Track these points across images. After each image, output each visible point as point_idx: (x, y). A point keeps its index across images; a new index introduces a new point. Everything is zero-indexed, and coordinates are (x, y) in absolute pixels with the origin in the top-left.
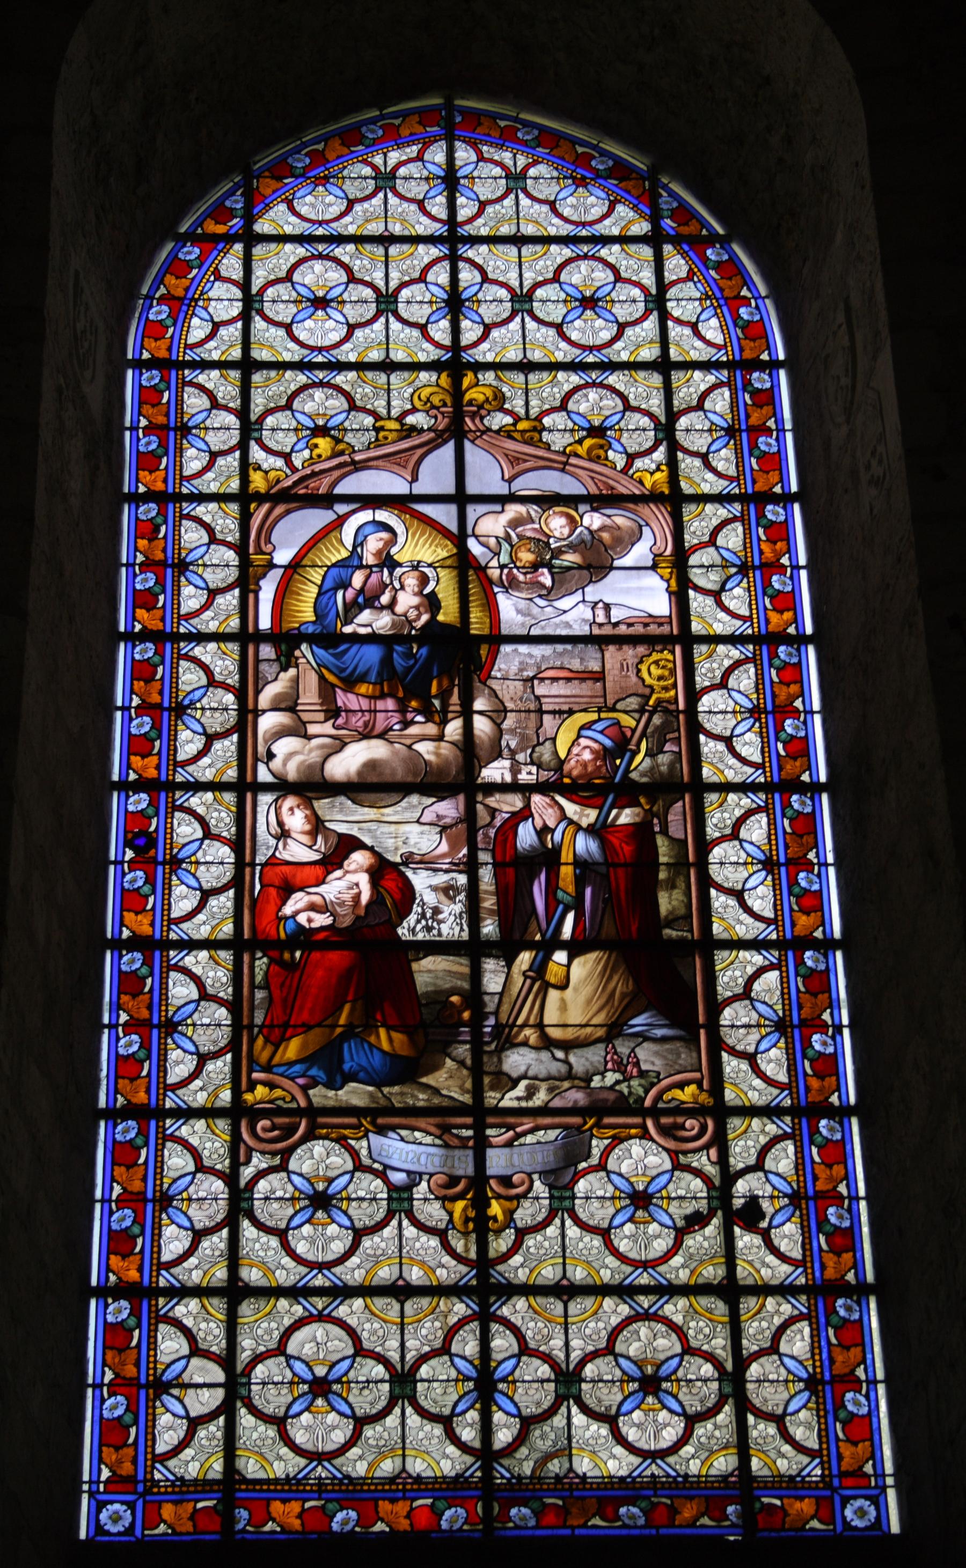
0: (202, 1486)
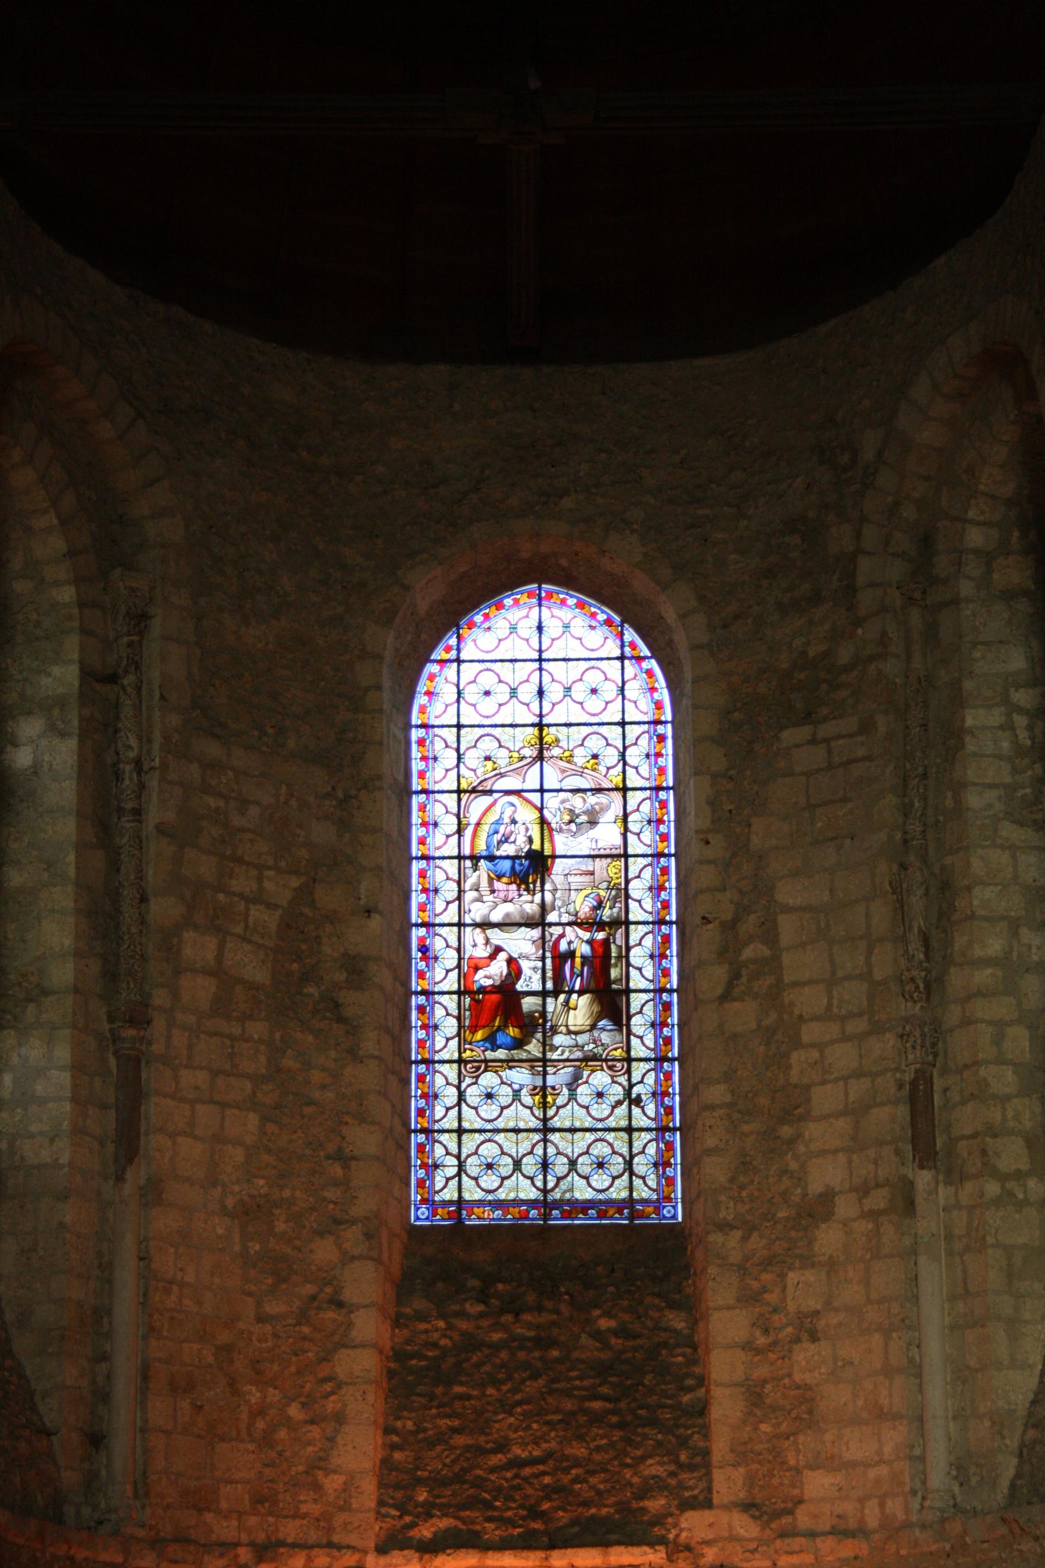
0: (451, 1202)
